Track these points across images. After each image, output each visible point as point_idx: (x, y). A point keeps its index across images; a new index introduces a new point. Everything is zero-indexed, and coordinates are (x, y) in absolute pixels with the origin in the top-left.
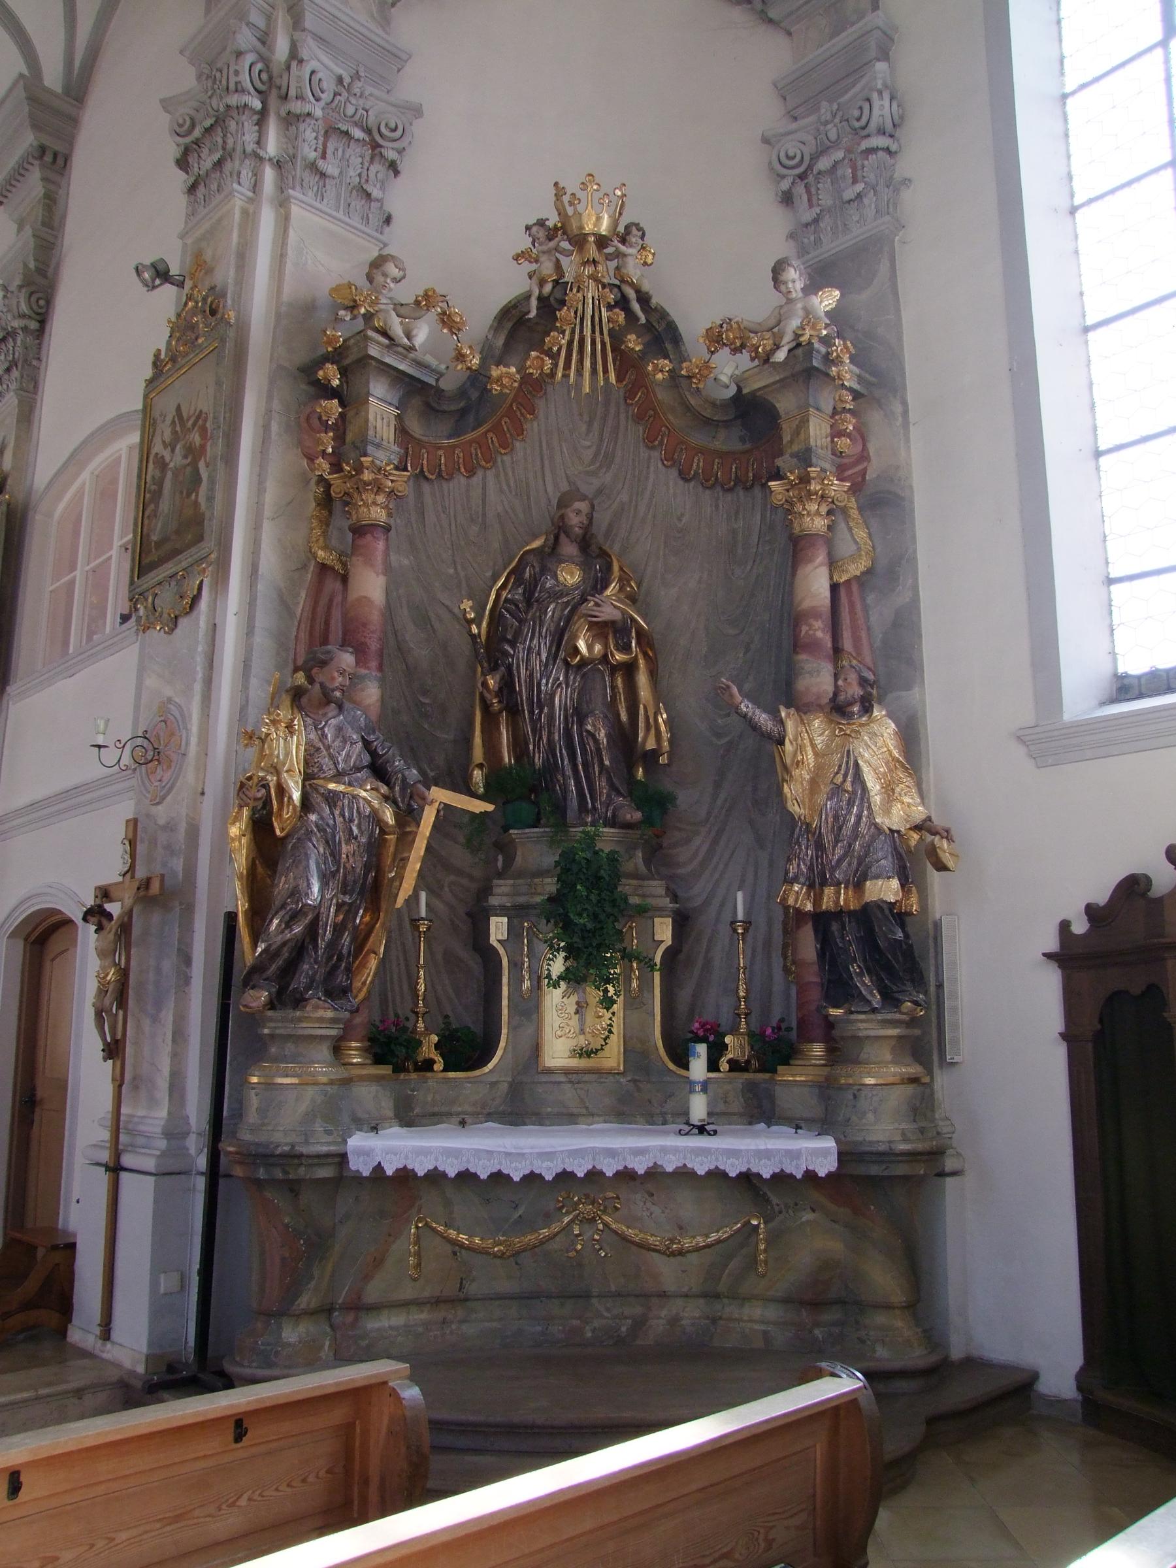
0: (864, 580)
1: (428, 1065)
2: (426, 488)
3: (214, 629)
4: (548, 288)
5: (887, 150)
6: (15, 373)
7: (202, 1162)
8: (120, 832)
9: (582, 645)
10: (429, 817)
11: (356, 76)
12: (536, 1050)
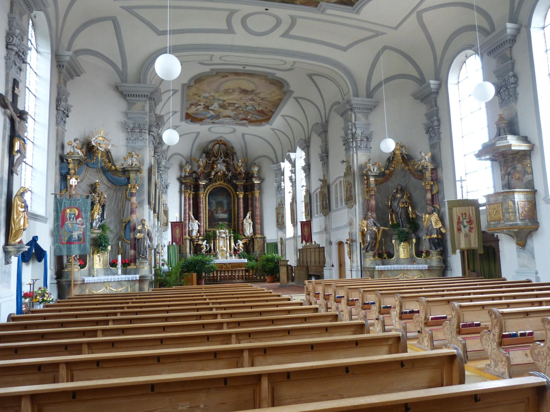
0: (438, 193)
1: (385, 258)
2: (380, 185)
3: (355, 209)
4: (393, 156)
5: (439, 129)
6: (325, 165)
7: (360, 270)
8: (348, 233)
9: (400, 206)
10: (381, 230)
11: (364, 131)
12: (399, 256)
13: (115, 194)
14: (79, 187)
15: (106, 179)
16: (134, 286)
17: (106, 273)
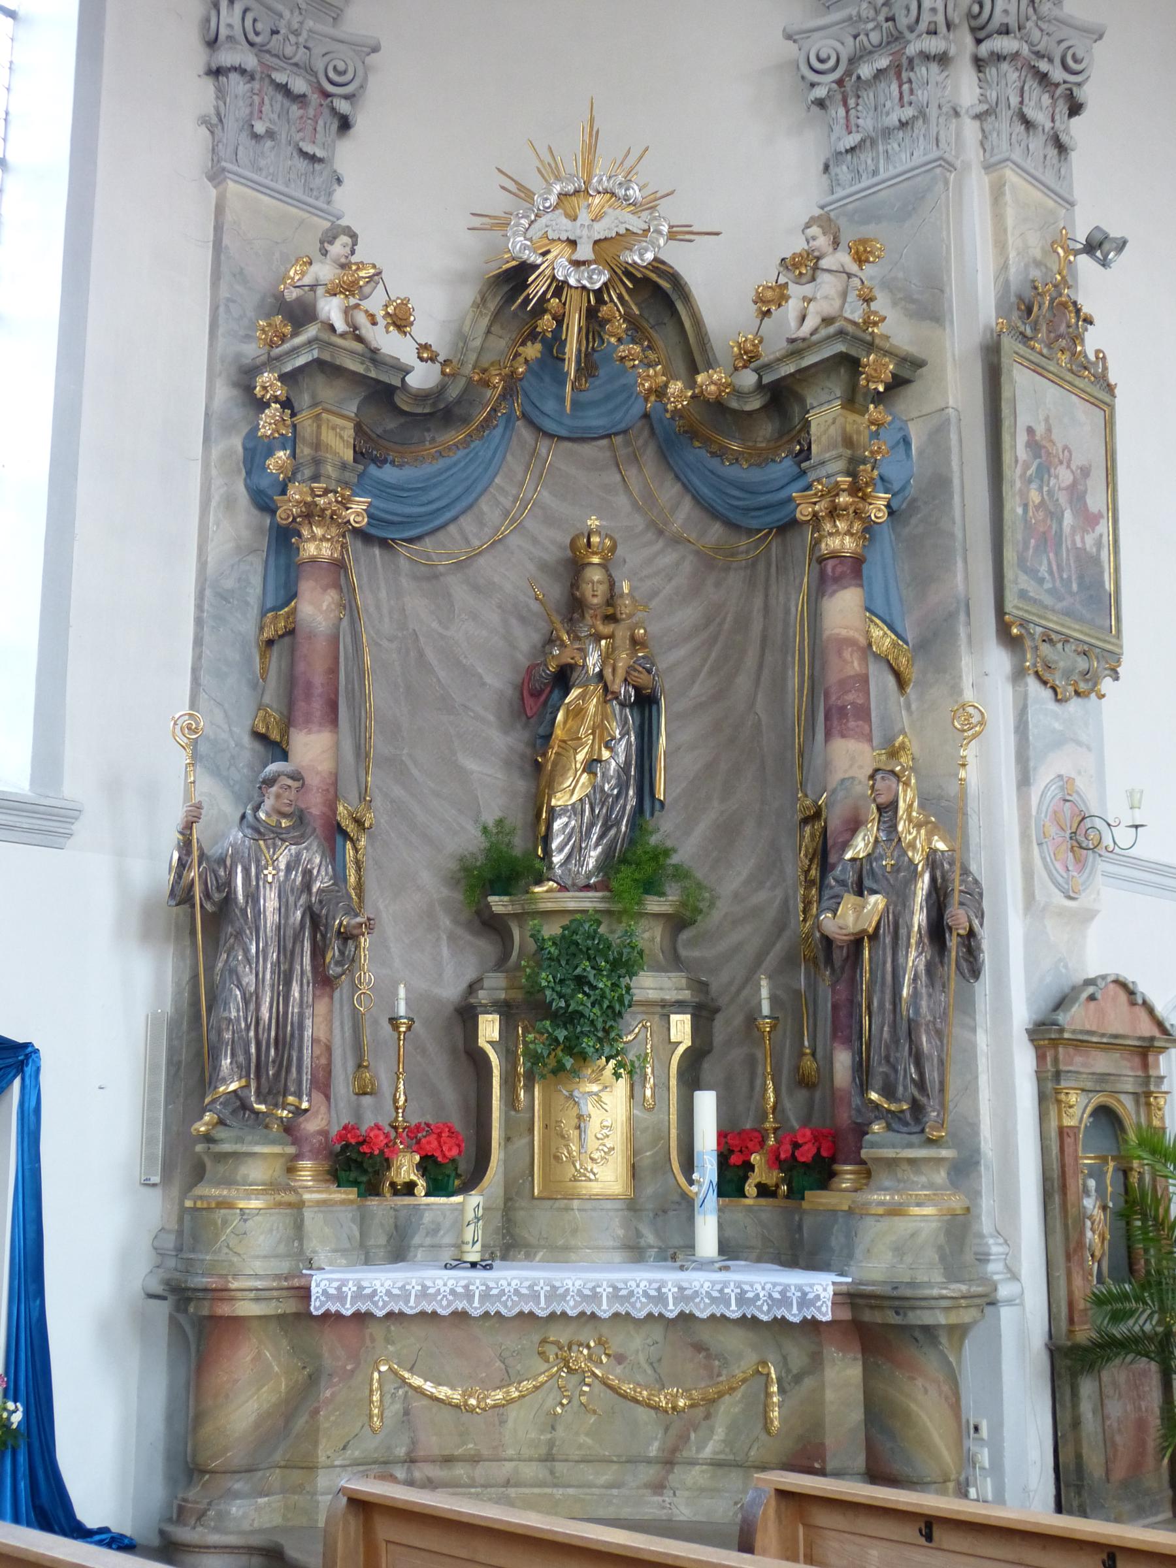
13: (758, 602)
14: (476, 588)
15: (687, 504)
16: (808, 1382)
17: (650, 1238)
